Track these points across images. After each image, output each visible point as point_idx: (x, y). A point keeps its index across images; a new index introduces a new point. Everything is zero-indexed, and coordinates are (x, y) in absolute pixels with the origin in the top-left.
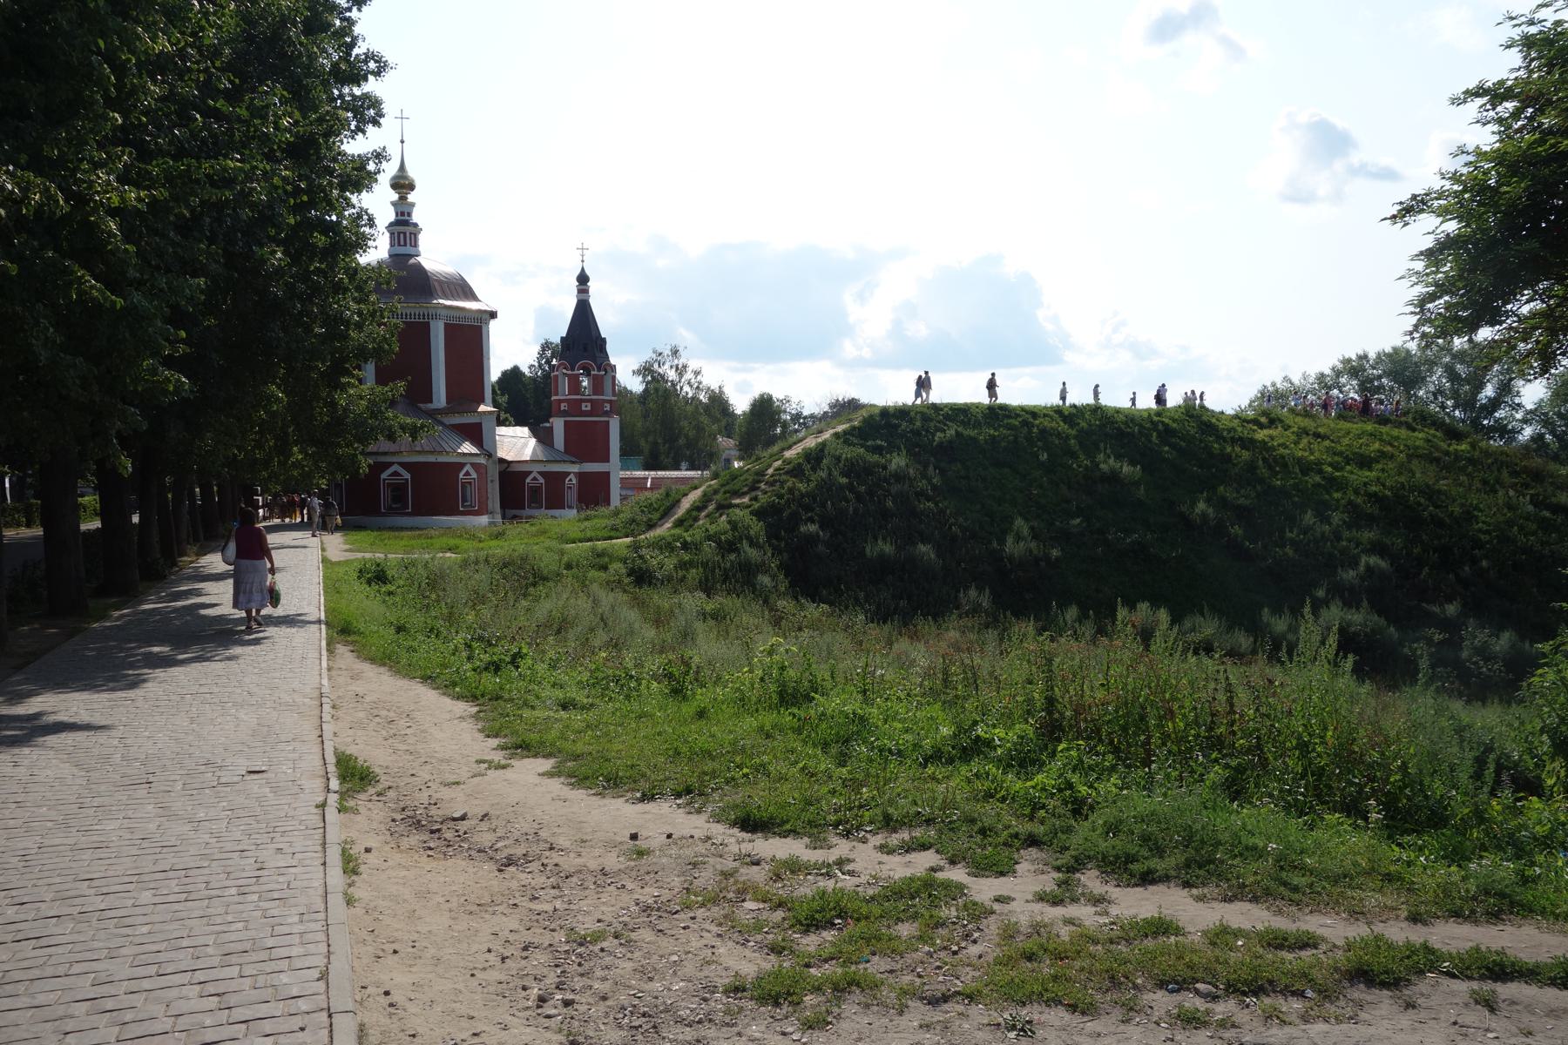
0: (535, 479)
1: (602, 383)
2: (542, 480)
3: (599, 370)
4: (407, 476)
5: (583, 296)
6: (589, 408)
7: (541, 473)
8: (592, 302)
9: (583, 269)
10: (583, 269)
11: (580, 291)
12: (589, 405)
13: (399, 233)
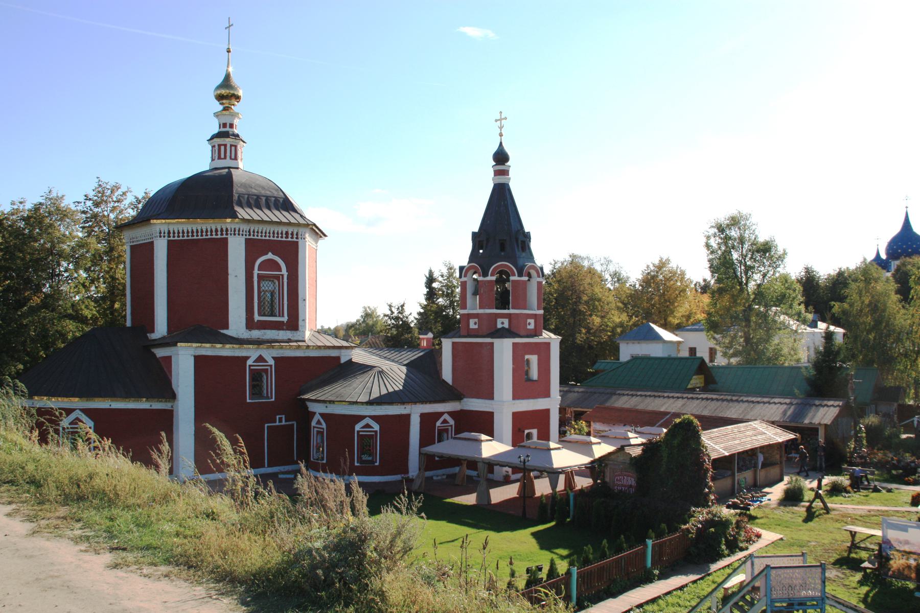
0: (367, 426)
1: (526, 288)
2: (376, 427)
3: (520, 275)
5: (501, 179)
6: (499, 321)
7: (373, 418)
9: (501, 144)
10: (501, 144)
11: (497, 173)
13: (220, 146)
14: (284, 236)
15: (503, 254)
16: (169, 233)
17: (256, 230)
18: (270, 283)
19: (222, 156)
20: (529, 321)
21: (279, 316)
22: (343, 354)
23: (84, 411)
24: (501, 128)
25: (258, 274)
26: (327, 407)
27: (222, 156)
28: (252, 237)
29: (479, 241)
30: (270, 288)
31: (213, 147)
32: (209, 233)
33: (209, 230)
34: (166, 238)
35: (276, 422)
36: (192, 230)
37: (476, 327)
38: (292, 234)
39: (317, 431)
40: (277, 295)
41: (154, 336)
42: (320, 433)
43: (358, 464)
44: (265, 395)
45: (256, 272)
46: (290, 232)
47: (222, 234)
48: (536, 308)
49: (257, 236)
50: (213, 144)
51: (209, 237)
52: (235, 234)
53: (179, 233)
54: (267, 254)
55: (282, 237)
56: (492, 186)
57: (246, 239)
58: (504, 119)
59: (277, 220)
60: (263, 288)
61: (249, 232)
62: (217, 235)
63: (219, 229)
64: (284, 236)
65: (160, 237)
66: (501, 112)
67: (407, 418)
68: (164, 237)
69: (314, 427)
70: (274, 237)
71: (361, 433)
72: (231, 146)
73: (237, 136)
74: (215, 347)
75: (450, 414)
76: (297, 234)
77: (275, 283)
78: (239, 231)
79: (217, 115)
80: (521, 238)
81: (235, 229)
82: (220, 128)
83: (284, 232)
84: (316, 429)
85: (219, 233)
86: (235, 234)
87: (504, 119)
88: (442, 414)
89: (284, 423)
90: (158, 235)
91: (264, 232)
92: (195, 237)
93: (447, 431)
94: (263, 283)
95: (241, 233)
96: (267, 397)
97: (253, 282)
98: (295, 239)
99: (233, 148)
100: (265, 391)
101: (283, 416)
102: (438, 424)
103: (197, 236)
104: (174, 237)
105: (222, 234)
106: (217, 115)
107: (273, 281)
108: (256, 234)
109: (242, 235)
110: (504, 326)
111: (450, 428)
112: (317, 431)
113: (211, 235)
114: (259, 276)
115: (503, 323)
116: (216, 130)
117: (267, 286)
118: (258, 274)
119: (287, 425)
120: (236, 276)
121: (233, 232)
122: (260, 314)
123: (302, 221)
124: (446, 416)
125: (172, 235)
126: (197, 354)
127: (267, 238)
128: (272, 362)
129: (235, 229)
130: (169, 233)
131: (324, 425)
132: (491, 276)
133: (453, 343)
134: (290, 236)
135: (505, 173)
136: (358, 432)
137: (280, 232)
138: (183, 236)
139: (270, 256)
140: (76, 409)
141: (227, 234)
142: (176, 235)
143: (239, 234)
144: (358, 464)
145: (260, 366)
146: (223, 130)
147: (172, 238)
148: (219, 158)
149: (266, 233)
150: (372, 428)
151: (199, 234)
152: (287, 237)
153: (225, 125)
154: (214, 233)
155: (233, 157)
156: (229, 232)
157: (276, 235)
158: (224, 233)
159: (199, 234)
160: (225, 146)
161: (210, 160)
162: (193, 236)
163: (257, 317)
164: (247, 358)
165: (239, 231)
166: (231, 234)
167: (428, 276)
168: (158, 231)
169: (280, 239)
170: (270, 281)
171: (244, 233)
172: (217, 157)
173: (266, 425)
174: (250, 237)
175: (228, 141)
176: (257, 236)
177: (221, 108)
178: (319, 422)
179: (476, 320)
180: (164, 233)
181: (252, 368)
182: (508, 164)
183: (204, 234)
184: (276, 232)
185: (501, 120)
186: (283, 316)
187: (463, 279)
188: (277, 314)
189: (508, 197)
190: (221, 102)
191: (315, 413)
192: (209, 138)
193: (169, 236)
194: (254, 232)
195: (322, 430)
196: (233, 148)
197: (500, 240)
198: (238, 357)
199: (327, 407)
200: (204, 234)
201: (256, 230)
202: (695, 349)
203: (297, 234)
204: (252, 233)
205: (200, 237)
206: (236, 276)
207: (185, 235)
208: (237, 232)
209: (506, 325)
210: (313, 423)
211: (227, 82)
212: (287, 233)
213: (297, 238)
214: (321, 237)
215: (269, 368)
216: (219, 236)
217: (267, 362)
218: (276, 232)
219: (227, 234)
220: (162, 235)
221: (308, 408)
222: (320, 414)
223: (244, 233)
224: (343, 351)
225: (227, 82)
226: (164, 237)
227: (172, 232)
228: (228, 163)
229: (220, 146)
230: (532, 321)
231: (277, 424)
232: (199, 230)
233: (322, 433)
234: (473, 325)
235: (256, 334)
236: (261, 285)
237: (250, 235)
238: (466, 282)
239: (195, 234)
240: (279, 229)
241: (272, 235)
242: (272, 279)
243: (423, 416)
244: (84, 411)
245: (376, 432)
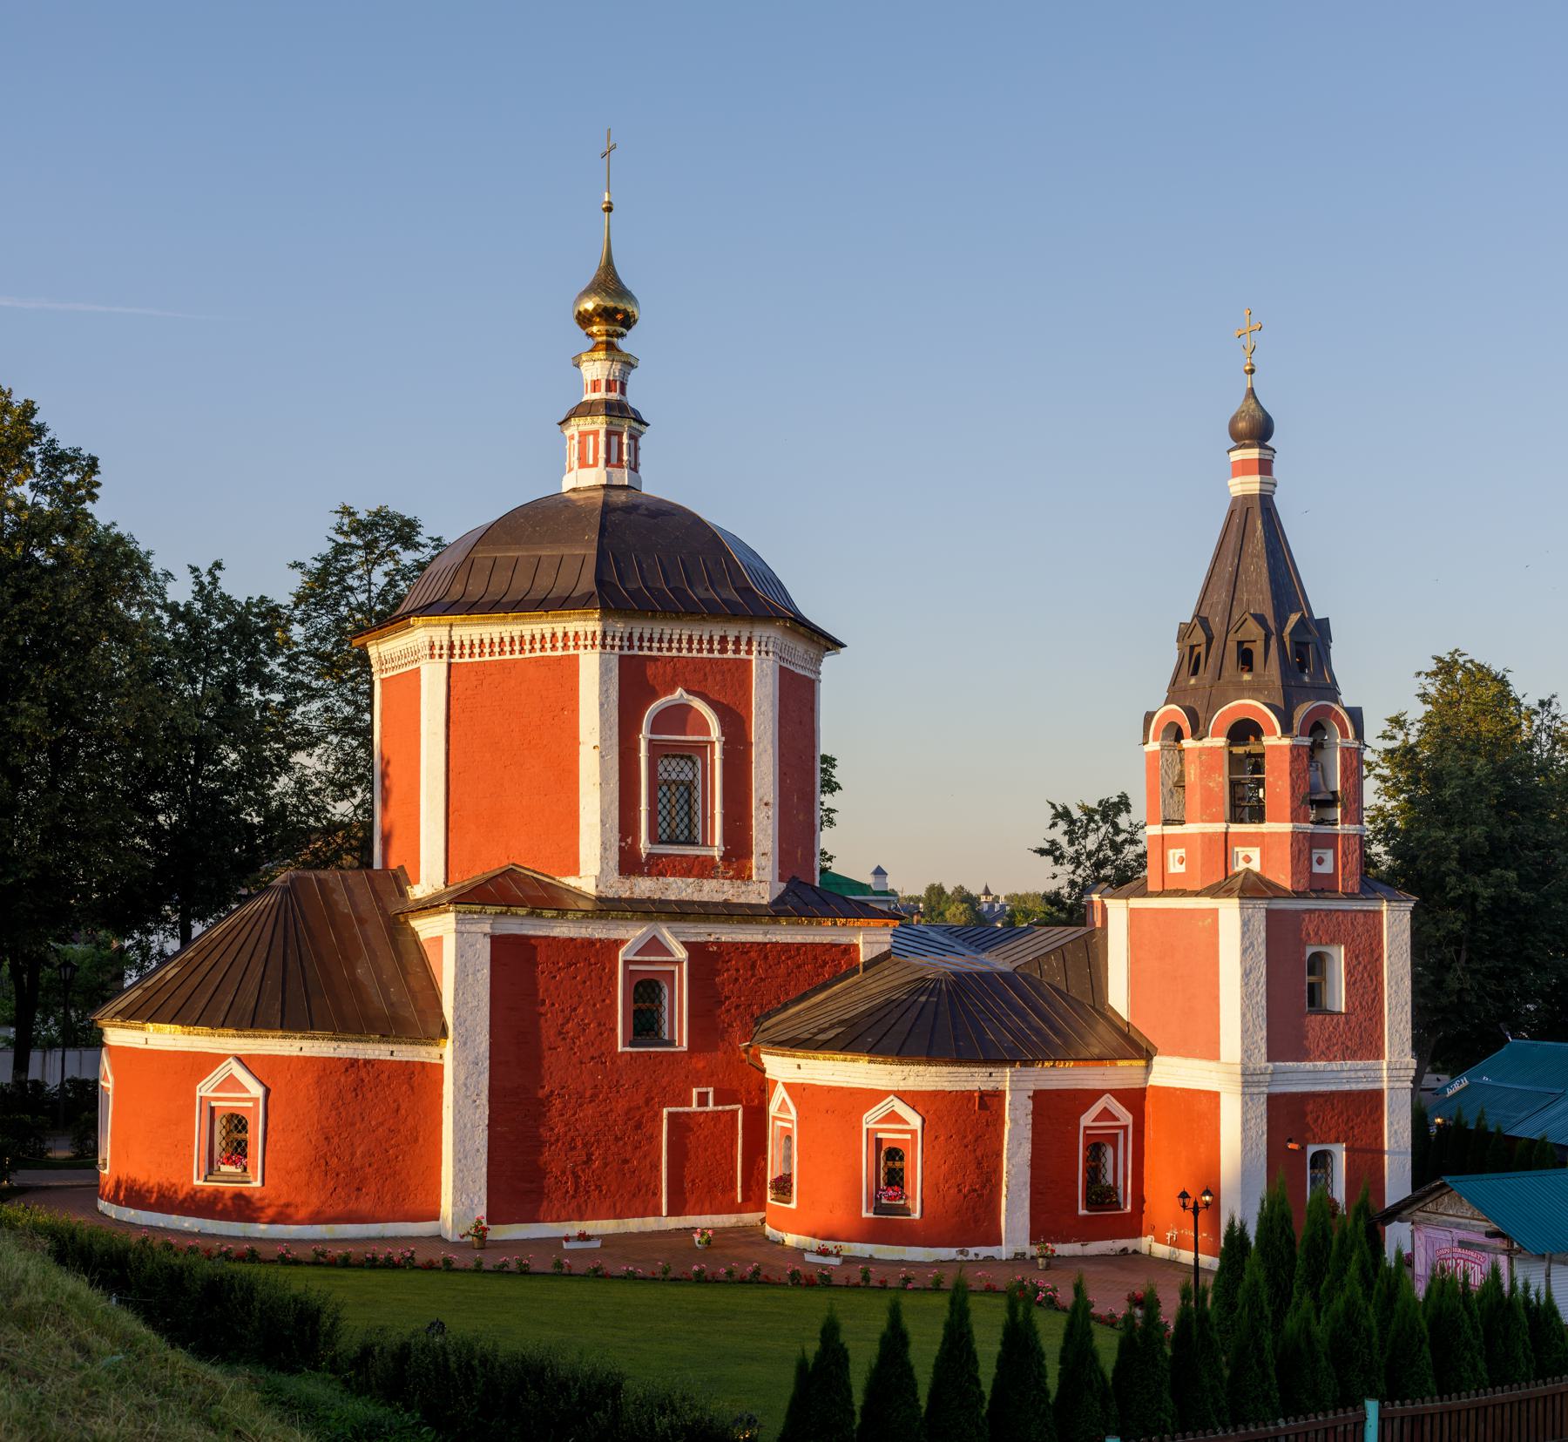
2: (915, 1121)
7: (910, 1098)
12: (1255, 853)
13: (583, 435)
14: (716, 646)
16: (451, 647)
17: (646, 636)
18: (682, 763)
21: (704, 844)
26: (799, 1067)
28: (636, 652)
30: (682, 776)
35: (691, 1106)
40: (698, 794)
41: (418, 892)
43: (871, 1215)
47: (565, 647)
49: (650, 649)
51: (538, 654)
53: (472, 646)
54: (672, 690)
55: (711, 650)
57: (622, 659)
60: (665, 775)
64: (716, 646)
68: (441, 656)
69: (775, 1118)
70: (690, 650)
74: (540, 916)
77: (694, 763)
83: (716, 638)
84: (779, 1123)
85: (560, 644)
86: (593, 646)
88: (1098, 1094)
89: (711, 1107)
90: (428, 652)
91: (666, 637)
92: (508, 656)
93: (1113, 1139)
94: (666, 762)
95: (609, 641)
96: (671, 1043)
100: (666, 1028)
101: (711, 1090)
102: (1087, 1120)
107: (689, 758)
108: (646, 644)
109: (613, 647)
113: (543, 648)
117: (673, 770)
119: (717, 1112)
121: (589, 642)
122: (654, 838)
127: (674, 653)
128: (681, 954)
130: (451, 647)
131: (793, 1116)
134: (730, 646)
138: (481, 654)
139: (679, 694)
141: (576, 647)
144: (871, 1215)
150: (906, 1123)
152: (723, 650)
154: (548, 645)
155: (614, 460)
156: (581, 643)
157: (695, 645)
158: (571, 643)
162: (502, 652)
163: (644, 845)
164: (618, 943)
166: (586, 647)
170: (682, 757)
171: (617, 642)
172: (576, 465)
173: (665, 1111)
174: (631, 653)
178: (783, 1107)
180: (441, 648)
181: (632, 967)
186: (713, 845)
188: (700, 840)
191: (776, 1082)
193: (451, 656)
194: (641, 639)
195: (789, 1125)
199: (799, 1067)
201: (646, 636)
204: (636, 643)
205: (517, 656)
210: (773, 1109)
211: (608, 281)
214: (828, 650)
216: (559, 653)
219: (576, 647)
220: (437, 652)
221: (764, 1071)
225: (608, 281)
226: (441, 656)
229: (583, 435)
231: (694, 1107)
235: (645, 887)
236: (661, 769)
237: (631, 647)
239: (507, 649)
241: (685, 645)
245: (913, 1132)
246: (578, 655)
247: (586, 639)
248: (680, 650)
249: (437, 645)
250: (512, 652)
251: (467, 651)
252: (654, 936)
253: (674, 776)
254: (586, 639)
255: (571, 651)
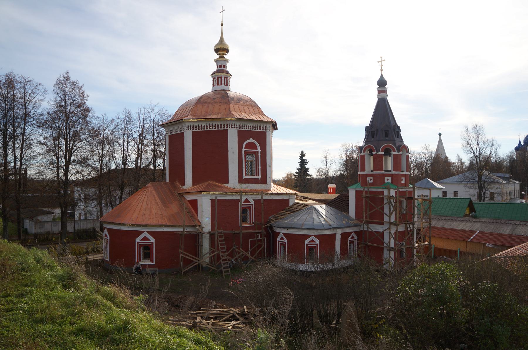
0: (312, 241)
1: (401, 159)
2: (318, 242)
4: (152, 240)
5: (382, 96)
6: (386, 178)
7: (316, 236)
8: (389, 99)
9: (382, 75)
10: (382, 75)
11: (380, 92)
15: (387, 139)
17: (243, 125)
19: (220, 83)
20: (402, 178)
21: (256, 175)
22: (290, 198)
23: (148, 232)
24: (382, 66)
25: (245, 151)
27: (220, 83)
28: (241, 129)
29: (372, 132)
30: (251, 159)
31: (214, 78)
32: (217, 127)
33: (217, 125)
34: (192, 129)
36: (207, 125)
37: (372, 182)
38: (263, 128)
39: (281, 244)
42: (283, 245)
44: (249, 222)
45: (244, 149)
46: (262, 126)
47: (224, 128)
48: (405, 170)
49: (244, 128)
50: (214, 77)
51: (217, 129)
52: (232, 127)
55: (257, 129)
56: (376, 100)
57: (239, 131)
58: (383, 61)
59: (256, 119)
61: (240, 126)
62: (221, 128)
63: (223, 125)
65: (188, 129)
66: (381, 57)
67: (334, 235)
68: (191, 129)
69: (279, 241)
70: (253, 129)
71: (308, 245)
72: (225, 77)
73: (227, 72)
75: (355, 232)
76: (265, 128)
78: (234, 125)
79: (216, 61)
80: (397, 130)
81: (232, 124)
82: (217, 68)
84: (279, 242)
85: (223, 127)
86: (232, 127)
87: (383, 61)
88: (351, 233)
90: (187, 128)
92: (209, 130)
94: (247, 156)
95: (235, 126)
97: (242, 155)
98: (264, 131)
99: (226, 79)
102: (349, 239)
103: (210, 128)
104: (196, 129)
105: (224, 128)
106: (216, 61)
108: (243, 127)
109: (236, 128)
110: (389, 181)
111: (355, 241)
112: (281, 244)
113: (218, 128)
114: (245, 152)
115: (388, 180)
116: (215, 69)
117: (249, 158)
118: (245, 151)
120: (233, 152)
121: (231, 126)
122: (246, 174)
123: (269, 120)
124: (353, 234)
125: (195, 128)
126: (212, 198)
127: (250, 130)
128: (253, 203)
129: (232, 124)
130: (193, 127)
131: (286, 241)
132: (381, 152)
133: (356, 191)
134: (262, 129)
135: (385, 92)
136: (307, 244)
137: (256, 126)
139: (251, 140)
140: (145, 231)
141: (227, 127)
142: (197, 128)
143: (234, 128)
145: (246, 205)
146: (219, 69)
147: (195, 130)
148: (218, 84)
149: (249, 127)
151: (211, 127)
152: (260, 129)
153: (220, 66)
154: (220, 127)
155: (226, 84)
156: (229, 126)
158: (226, 127)
159: (211, 127)
160: (221, 78)
161: (212, 86)
162: (207, 129)
163: (244, 176)
165: (234, 125)
166: (230, 127)
167: (301, 153)
168: (187, 126)
169: (256, 130)
171: (237, 127)
172: (216, 84)
173: (250, 240)
174: (240, 129)
175: (223, 75)
176: (244, 128)
177: (218, 57)
178: (282, 238)
179: (372, 178)
180: (191, 127)
182: (386, 87)
183: (214, 127)
184: (254, 126)
185: (381, 61)
186: (258, 175)
187: (363, 154)
189: (387, 105)
190: (218, 53)
191: (280, 233)
192: (211, 74)
193: (193, 129)
194: (242, 126)
195: (284, 243)
196: (226, 79)
197: (385, 131)
198: (234, 200)
200: (214, 127)
201: (243, 125)
202: (446, 192)
203: (265, 128)
204: (241, 127)
205: (211, 129)
206: (233, 152)
207: (203, 128)
208: (233, 126)
209: (390, 181)
210: (278, 239)
212: (260, 127)
213: (265, 130)
215: (251, 206)
216: (223, 129)
217: (250, 203)
218: (254, 126)
219: (227, 127)
220: (189, 128)
222: (283, 234)
223: (237, 127)
224: (291, 196)
226: (191, 129)
227: (195, 126)
228: (223, 87)
229: (218, 78)
230: (403, 179)
232: (211, 125)
233: (285, 245)
234: (370, 180)
235: (244, 186)
237: (240, 128)
238: (364, 155)
239: (208, 128)
240: (255, 125)
242: (252, 154)
243: (342, 234)
244: (148, 232)
245: (317, 244)
246: (228, 130)
247: (230, 126)
248: (251, 129)
249: (189, 126)
250: (210, 128)
251: (197, 128)
252: (247, 199)
253: (249, 159)
254: (230, 126)
255: (226, 129)
